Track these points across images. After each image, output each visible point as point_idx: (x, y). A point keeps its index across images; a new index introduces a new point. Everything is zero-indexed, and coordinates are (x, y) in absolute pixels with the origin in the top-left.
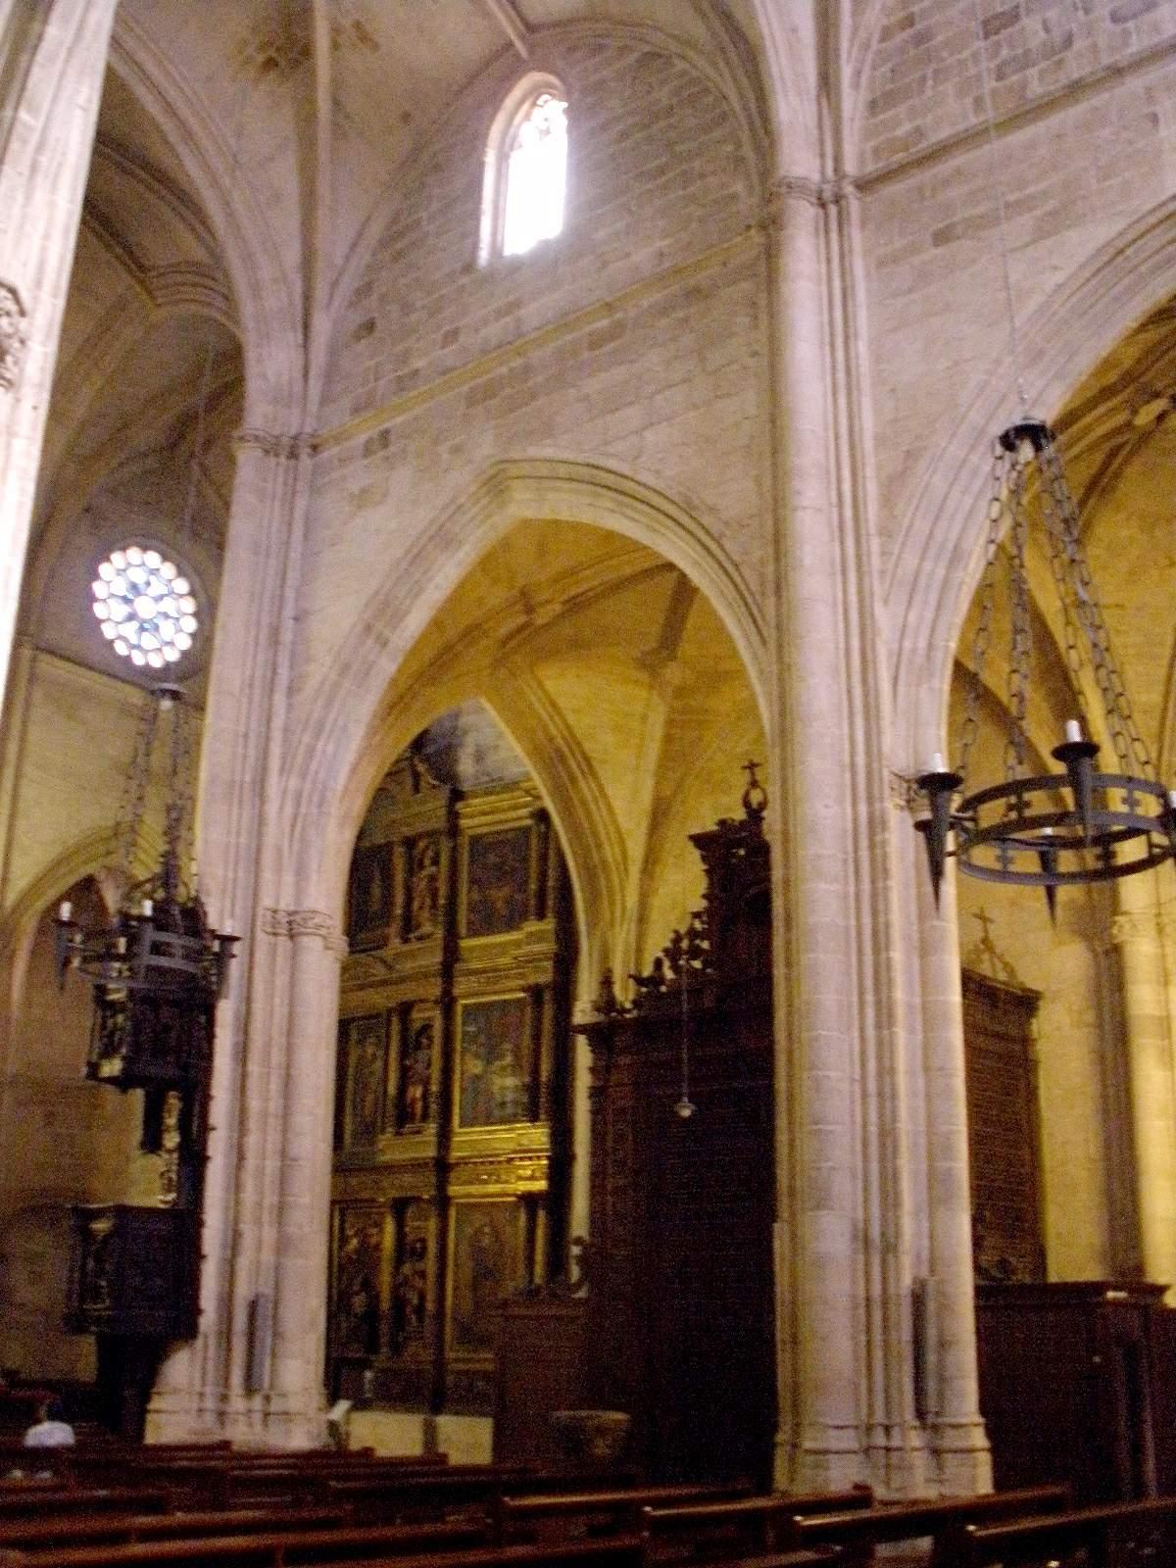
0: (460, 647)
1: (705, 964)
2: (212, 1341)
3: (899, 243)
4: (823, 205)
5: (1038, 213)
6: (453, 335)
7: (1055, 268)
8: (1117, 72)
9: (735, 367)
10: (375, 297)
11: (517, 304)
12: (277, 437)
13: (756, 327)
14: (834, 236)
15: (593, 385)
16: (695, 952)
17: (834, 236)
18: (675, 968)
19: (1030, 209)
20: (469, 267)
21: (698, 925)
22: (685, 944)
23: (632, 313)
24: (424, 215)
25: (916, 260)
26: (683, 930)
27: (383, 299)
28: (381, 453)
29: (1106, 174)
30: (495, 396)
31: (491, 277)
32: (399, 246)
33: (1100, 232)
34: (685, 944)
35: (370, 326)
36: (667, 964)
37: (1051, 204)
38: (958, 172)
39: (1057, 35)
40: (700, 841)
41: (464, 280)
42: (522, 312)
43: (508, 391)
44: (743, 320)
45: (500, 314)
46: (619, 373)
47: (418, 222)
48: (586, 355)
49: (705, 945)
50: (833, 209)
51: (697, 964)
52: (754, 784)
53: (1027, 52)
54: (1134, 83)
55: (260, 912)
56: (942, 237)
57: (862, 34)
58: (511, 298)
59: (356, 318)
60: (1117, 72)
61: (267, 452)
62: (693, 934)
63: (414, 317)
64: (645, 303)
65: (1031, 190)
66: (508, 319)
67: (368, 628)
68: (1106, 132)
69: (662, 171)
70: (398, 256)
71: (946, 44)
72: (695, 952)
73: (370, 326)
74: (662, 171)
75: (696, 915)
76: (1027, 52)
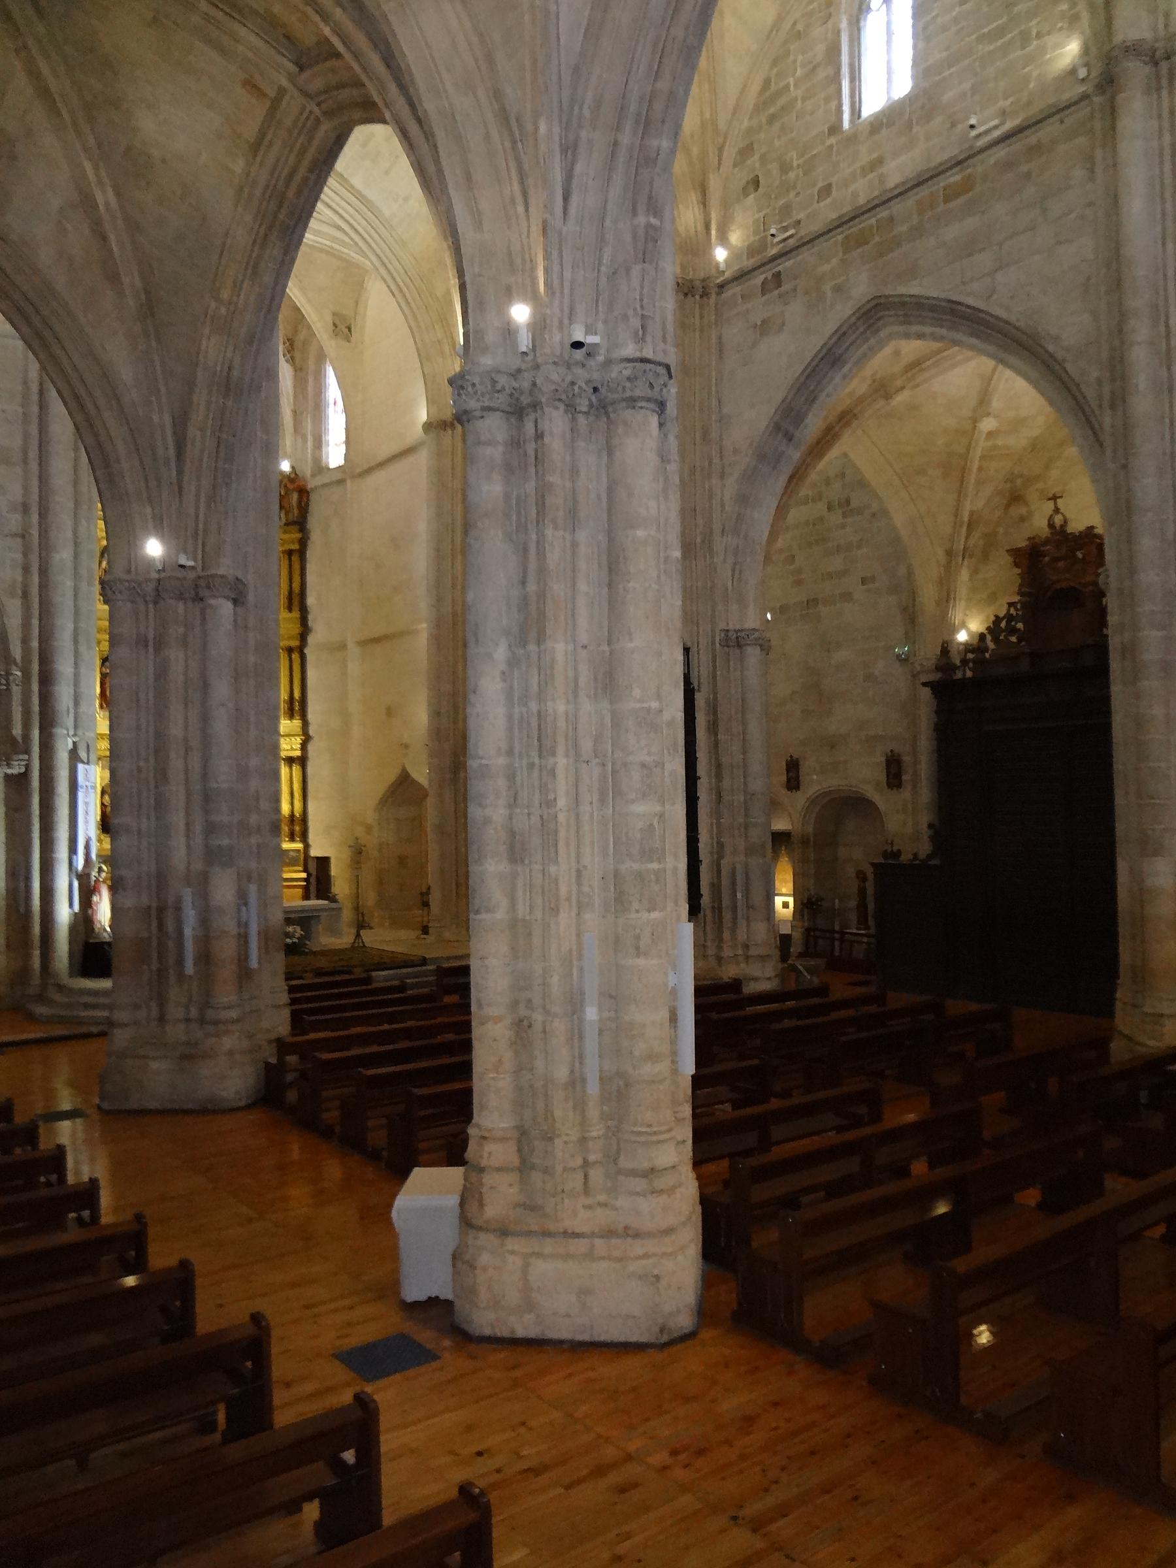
0: (837, 429)
1: (1020, 640)
2: (709, 914)
4: (1156, 64)
6: (826, 191)
9: (1073, 216)
10: (757, 156)
11: (880, 161)
12: (691, 281)
13: (1092, 179)
14: (1165, 93)
15: (953, 232)
16: (1012, 631)
17: (1165, 93)
18: (996, 640)
20: (835, 128)
21: (1012, 611)
22: (1003, 624)
23: (980, 169)
24: (791, 80)
26: (1001, 615)
27: (764, 159)
28: (776, 292)
30: (867, 243)
31: (852, 139)
32: (772, 110)
34: (1003, 624)
35: (756, 183)
36: (989, 638)
40: (1015, 553)
41: (832, 140)
42: (883, 170)
43: (877, 239)
44: (1078, 173)
45: (864, 171)
46: (972, 222)
47: (787, 86)
48: (941, 207)
49: (1020, 626)
50: (1164, 66)
51: (1014, 639)
52: (1057, 510)
55: (717, 631)
58: (875, 155)
59: (741, 177)
61: (686, 295)
62: (1009, 618)
63: (792, 175)
64: (992, 161)
66: (871, 176)
67: (777, 427)
69: (1001, 32)
70: (772, 119)
72: (1012, 631)
73: (756, 183)
74: (1001, 32)
75: (1010, 605)
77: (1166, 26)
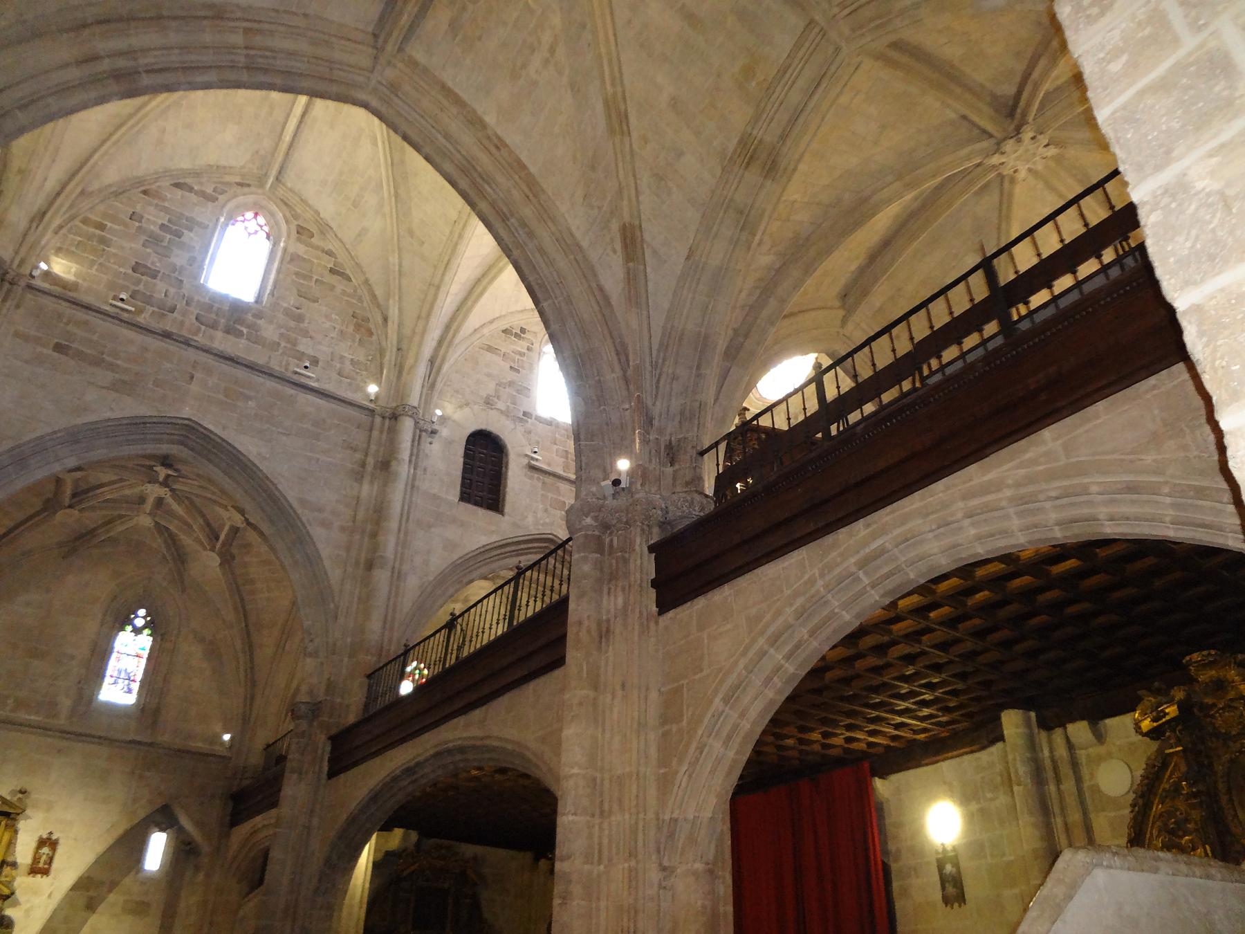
3: (33, 333)
5: (117, 376)
7: (112, 409)
8: (187, 343)
19: (113, 371)
25: (39, 349)
29: (157, 383)
33: (143, 410)
37: (126, 378)
38: (86, 323)
39: (169, 303)
53: (151, 296)
54: (191, 354)
56: (59, 348)
57: (74, 211)
60: (187, 343)
65: (119, 362)
68: (168, 365)
71: (115, 255)
76: (151, 296)
77: (19, 266)
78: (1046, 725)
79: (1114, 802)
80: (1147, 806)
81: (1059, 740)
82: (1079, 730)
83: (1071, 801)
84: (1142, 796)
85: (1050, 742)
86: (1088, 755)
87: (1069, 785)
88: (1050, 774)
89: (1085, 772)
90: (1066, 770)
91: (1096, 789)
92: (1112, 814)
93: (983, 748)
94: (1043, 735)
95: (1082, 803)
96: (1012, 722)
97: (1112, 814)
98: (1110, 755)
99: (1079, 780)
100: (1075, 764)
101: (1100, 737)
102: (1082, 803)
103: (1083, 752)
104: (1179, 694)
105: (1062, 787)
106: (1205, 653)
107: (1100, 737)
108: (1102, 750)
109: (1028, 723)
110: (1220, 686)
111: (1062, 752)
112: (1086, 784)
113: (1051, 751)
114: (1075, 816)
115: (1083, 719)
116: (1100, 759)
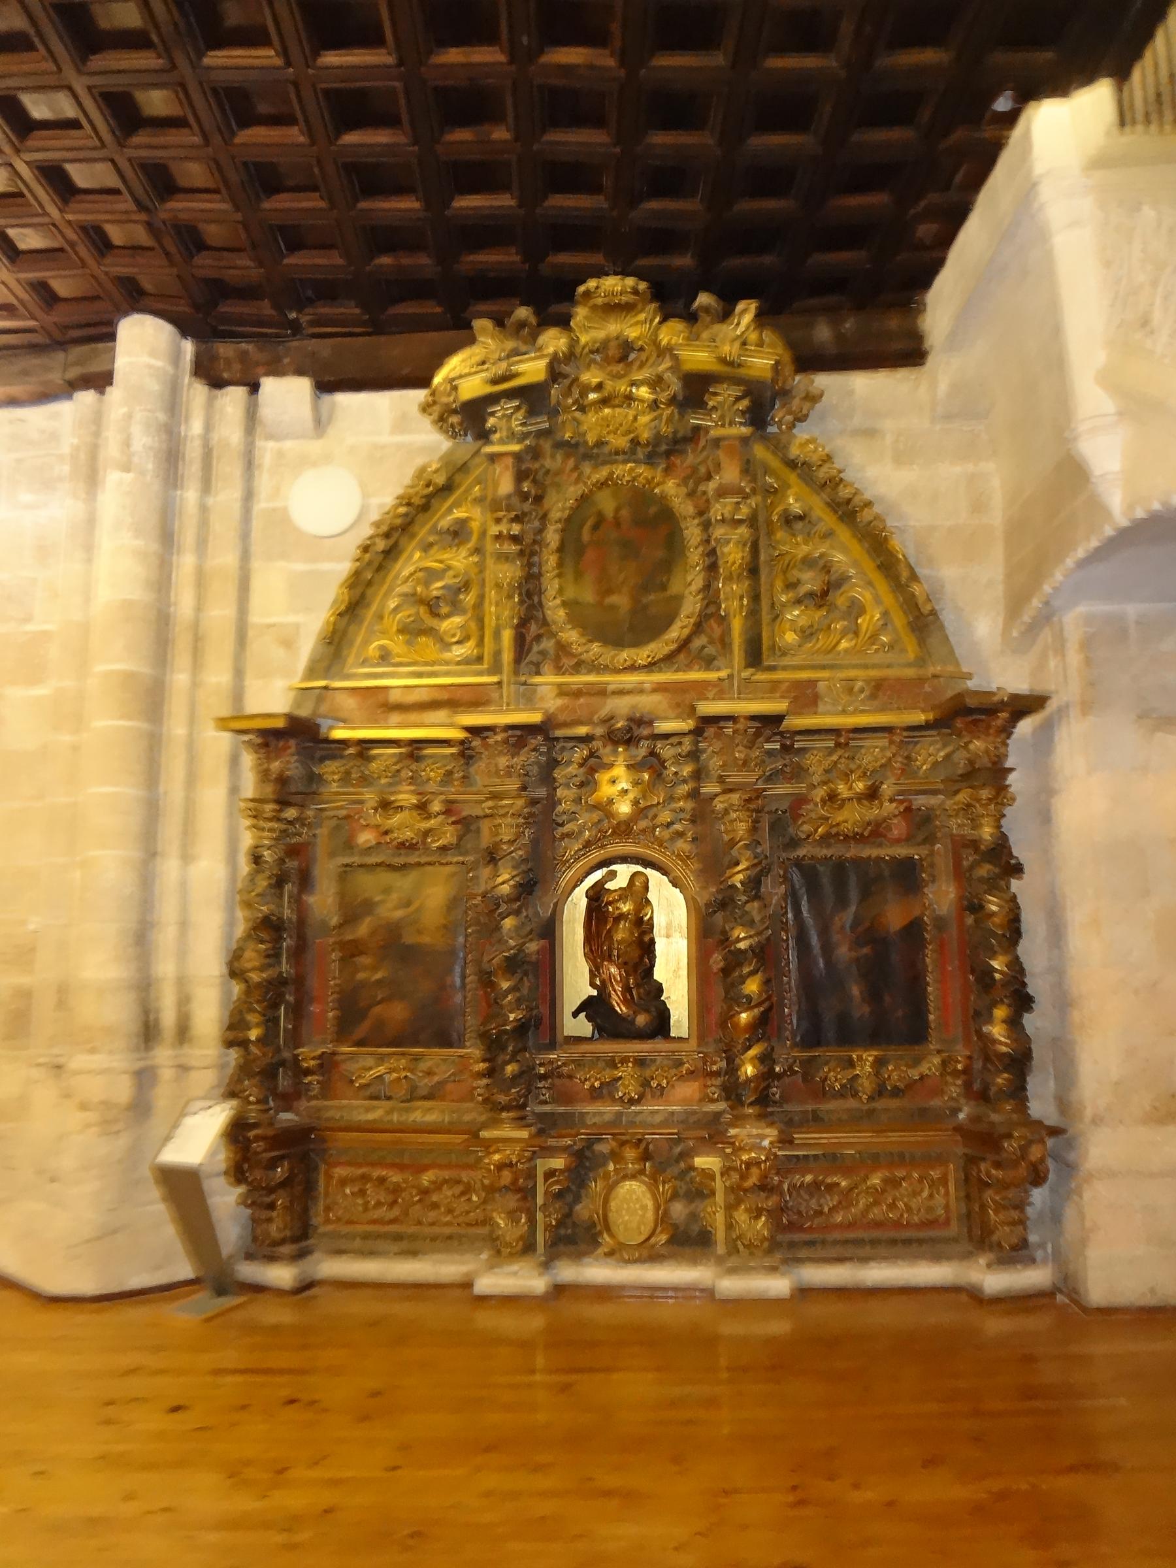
78: (211, 374)
79: (313, 546)
80: (391, 553)
81: (229, 409)
82: (286, 394)
83: (224, 527)
84: (387, 535)
85: (210, 404)
86: (280, 454)
87: (227, 497)
88: (192, 468)
89: (264, 482)
90: (229, 469)
91: (281, 518)
92: (300, 567)
93: (43, 397)
94: (199, 391)
95: (245, 536)
96: (144, 345)
97: (300, 567)
98: (327, 459)
99: (249, 496)
100: (249, 463)
101: (320, 424)
102: (245, 536)
103: (271, 444)
104: (553, 341)
105: (210, 501)
106: (630, 281)
107: (320, 424)
108: (314, 447)
109: (176, 358)
110: (623, 353)
111: (231, 431)
112: (261, 505)
113: (208, 427)
114: (225, 558)
115: (300, 372)
116: (304, 463)
